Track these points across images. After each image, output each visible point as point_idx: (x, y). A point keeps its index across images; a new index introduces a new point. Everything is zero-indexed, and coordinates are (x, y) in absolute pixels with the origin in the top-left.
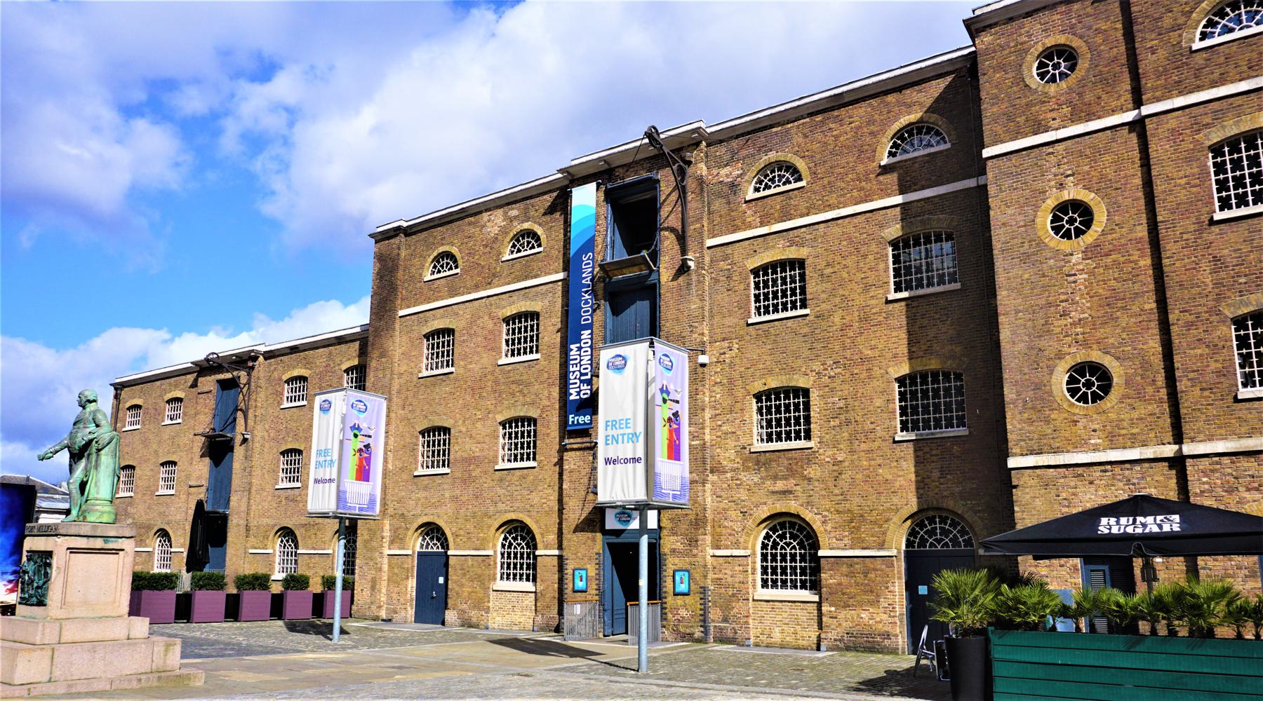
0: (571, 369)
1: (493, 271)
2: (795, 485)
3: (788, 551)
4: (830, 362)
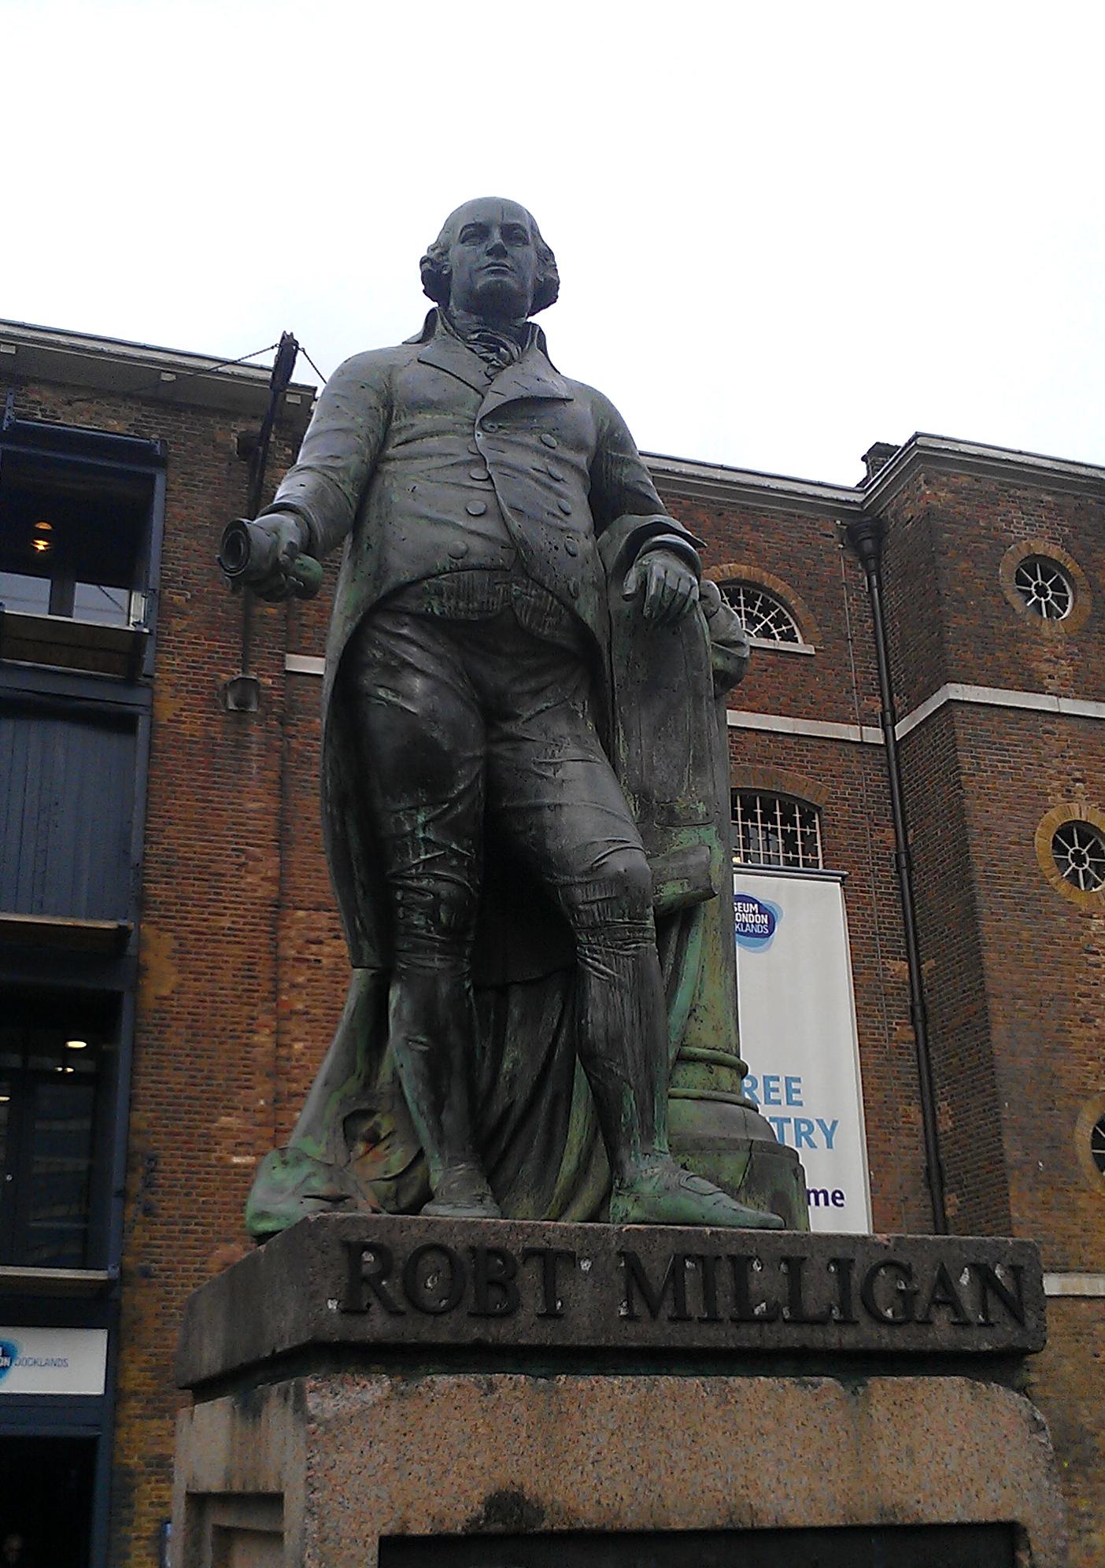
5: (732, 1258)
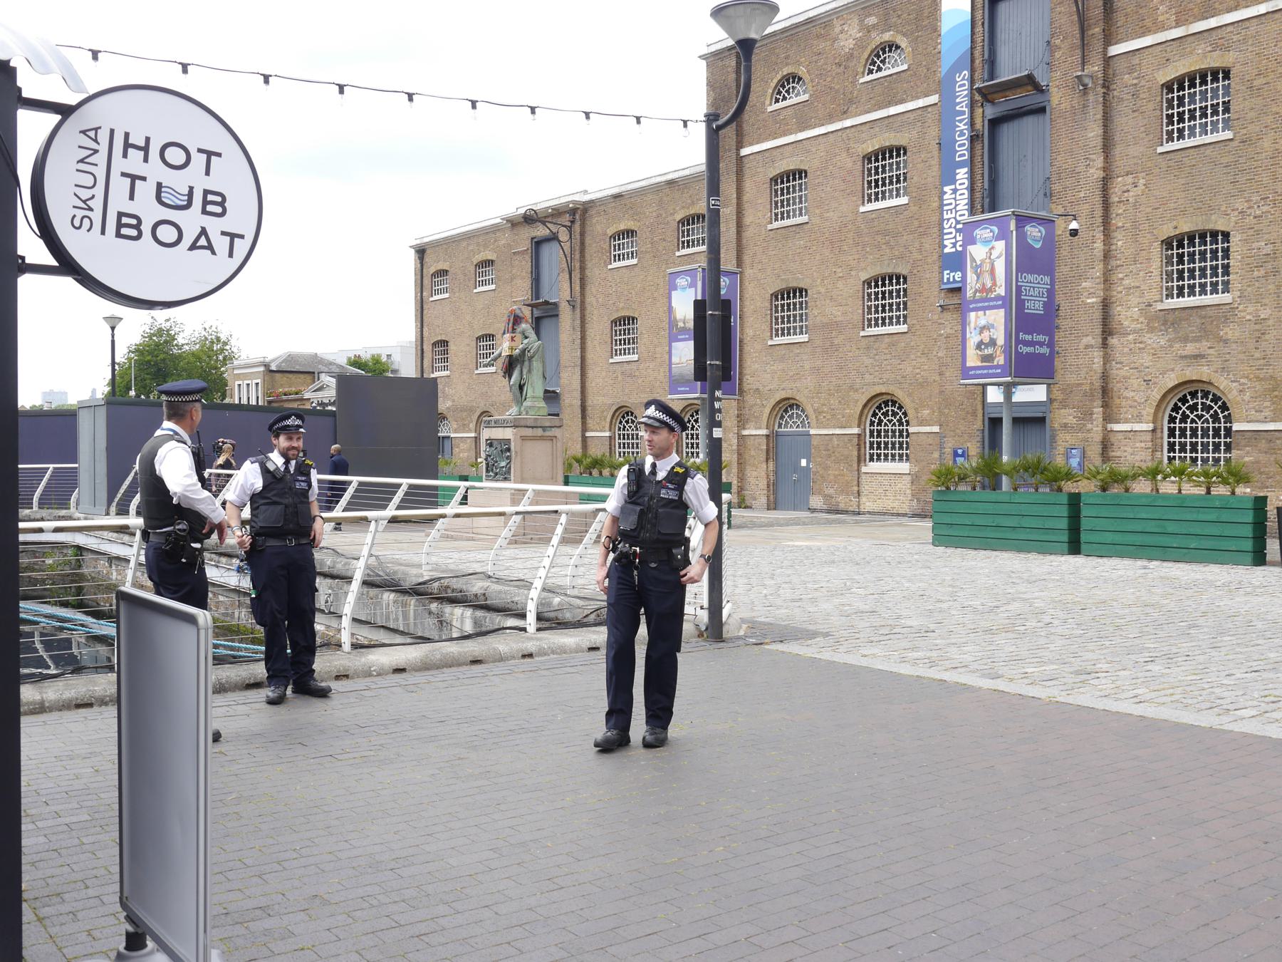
0: (946, 217)
1: (850, 96)
2: (1209, 348)
4: (1255, 198)
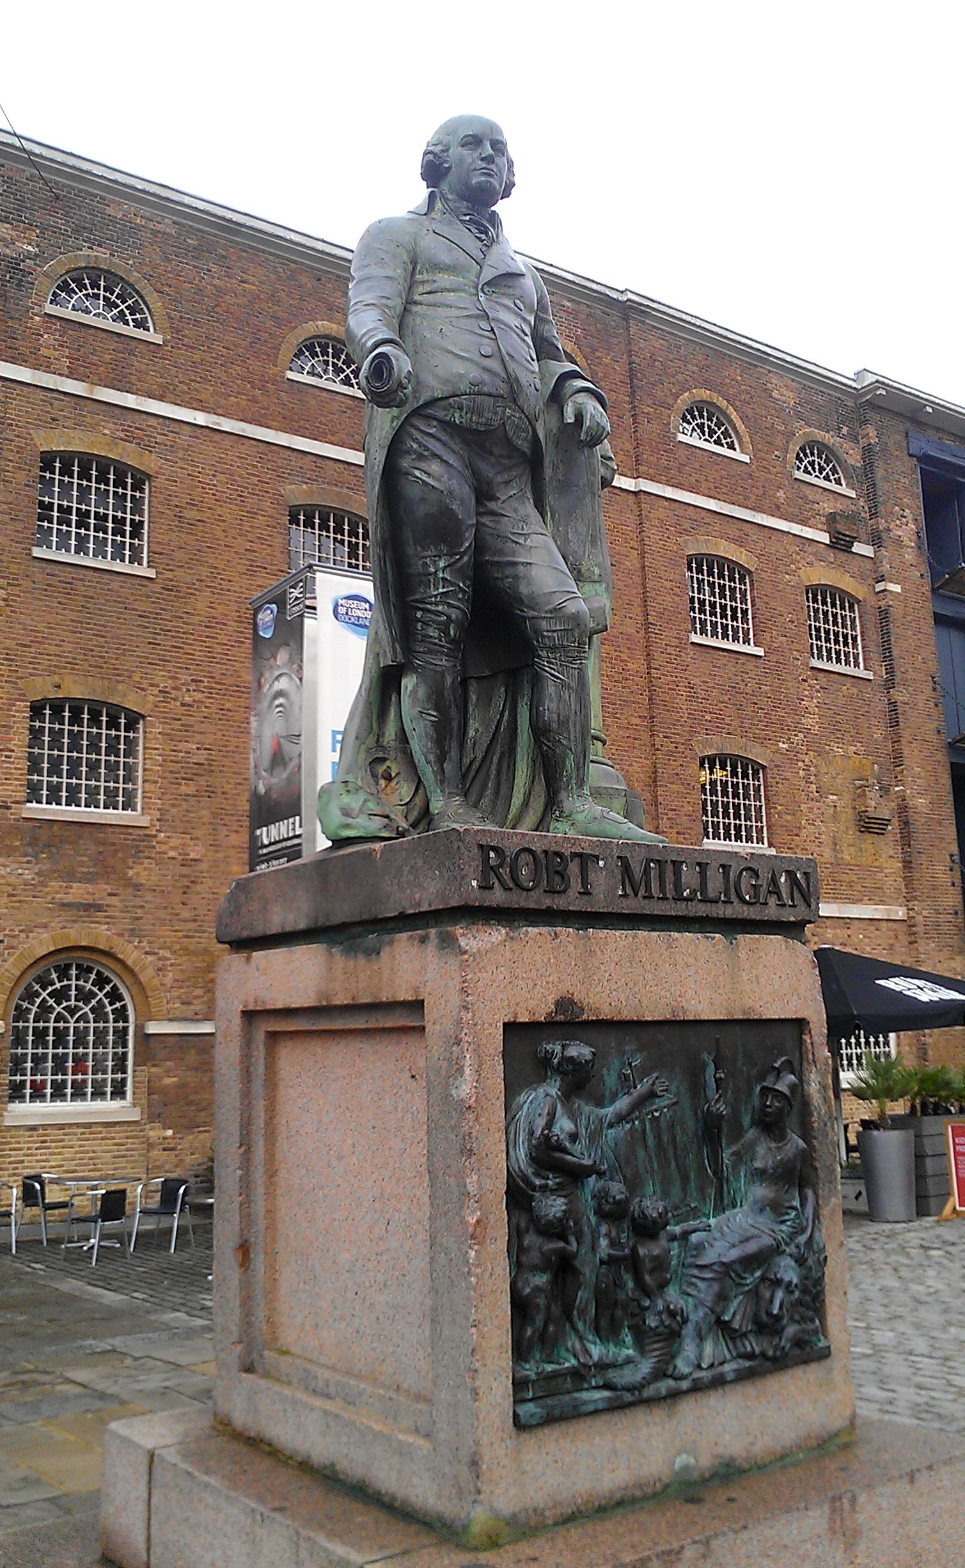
2: (110, 895)
3: (72, 1025)
4: (184, 677)
5: (673, 862)
